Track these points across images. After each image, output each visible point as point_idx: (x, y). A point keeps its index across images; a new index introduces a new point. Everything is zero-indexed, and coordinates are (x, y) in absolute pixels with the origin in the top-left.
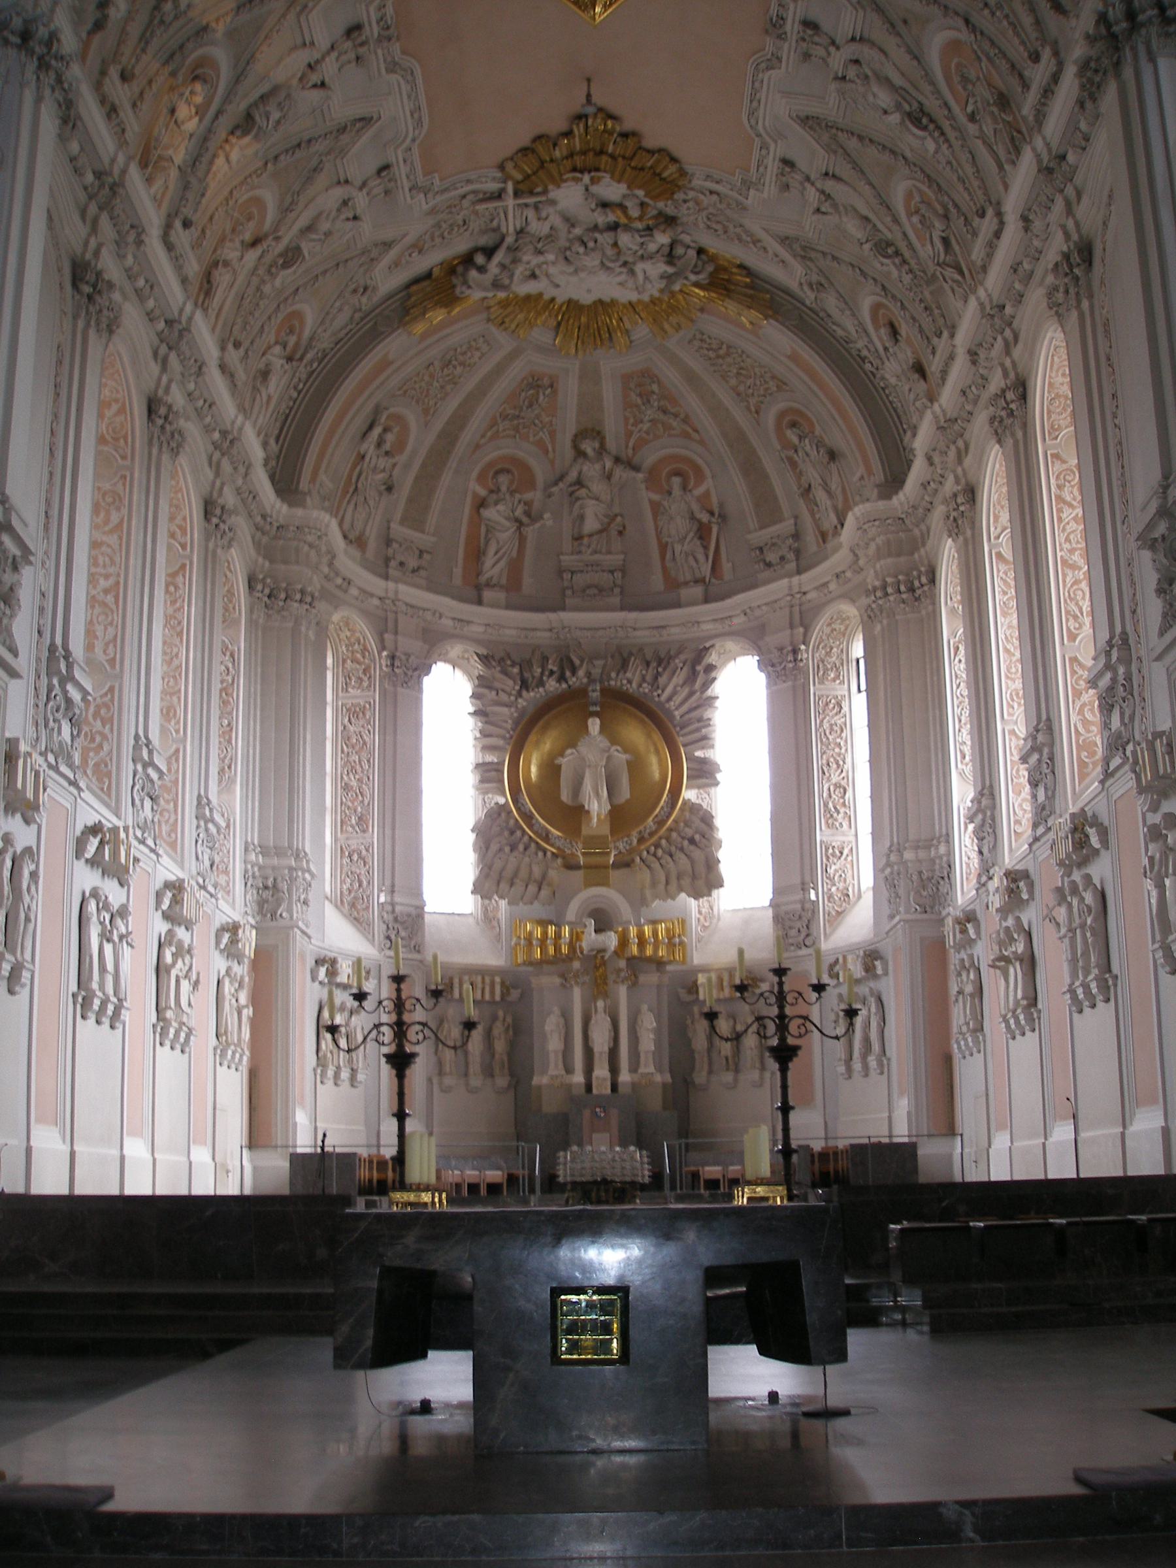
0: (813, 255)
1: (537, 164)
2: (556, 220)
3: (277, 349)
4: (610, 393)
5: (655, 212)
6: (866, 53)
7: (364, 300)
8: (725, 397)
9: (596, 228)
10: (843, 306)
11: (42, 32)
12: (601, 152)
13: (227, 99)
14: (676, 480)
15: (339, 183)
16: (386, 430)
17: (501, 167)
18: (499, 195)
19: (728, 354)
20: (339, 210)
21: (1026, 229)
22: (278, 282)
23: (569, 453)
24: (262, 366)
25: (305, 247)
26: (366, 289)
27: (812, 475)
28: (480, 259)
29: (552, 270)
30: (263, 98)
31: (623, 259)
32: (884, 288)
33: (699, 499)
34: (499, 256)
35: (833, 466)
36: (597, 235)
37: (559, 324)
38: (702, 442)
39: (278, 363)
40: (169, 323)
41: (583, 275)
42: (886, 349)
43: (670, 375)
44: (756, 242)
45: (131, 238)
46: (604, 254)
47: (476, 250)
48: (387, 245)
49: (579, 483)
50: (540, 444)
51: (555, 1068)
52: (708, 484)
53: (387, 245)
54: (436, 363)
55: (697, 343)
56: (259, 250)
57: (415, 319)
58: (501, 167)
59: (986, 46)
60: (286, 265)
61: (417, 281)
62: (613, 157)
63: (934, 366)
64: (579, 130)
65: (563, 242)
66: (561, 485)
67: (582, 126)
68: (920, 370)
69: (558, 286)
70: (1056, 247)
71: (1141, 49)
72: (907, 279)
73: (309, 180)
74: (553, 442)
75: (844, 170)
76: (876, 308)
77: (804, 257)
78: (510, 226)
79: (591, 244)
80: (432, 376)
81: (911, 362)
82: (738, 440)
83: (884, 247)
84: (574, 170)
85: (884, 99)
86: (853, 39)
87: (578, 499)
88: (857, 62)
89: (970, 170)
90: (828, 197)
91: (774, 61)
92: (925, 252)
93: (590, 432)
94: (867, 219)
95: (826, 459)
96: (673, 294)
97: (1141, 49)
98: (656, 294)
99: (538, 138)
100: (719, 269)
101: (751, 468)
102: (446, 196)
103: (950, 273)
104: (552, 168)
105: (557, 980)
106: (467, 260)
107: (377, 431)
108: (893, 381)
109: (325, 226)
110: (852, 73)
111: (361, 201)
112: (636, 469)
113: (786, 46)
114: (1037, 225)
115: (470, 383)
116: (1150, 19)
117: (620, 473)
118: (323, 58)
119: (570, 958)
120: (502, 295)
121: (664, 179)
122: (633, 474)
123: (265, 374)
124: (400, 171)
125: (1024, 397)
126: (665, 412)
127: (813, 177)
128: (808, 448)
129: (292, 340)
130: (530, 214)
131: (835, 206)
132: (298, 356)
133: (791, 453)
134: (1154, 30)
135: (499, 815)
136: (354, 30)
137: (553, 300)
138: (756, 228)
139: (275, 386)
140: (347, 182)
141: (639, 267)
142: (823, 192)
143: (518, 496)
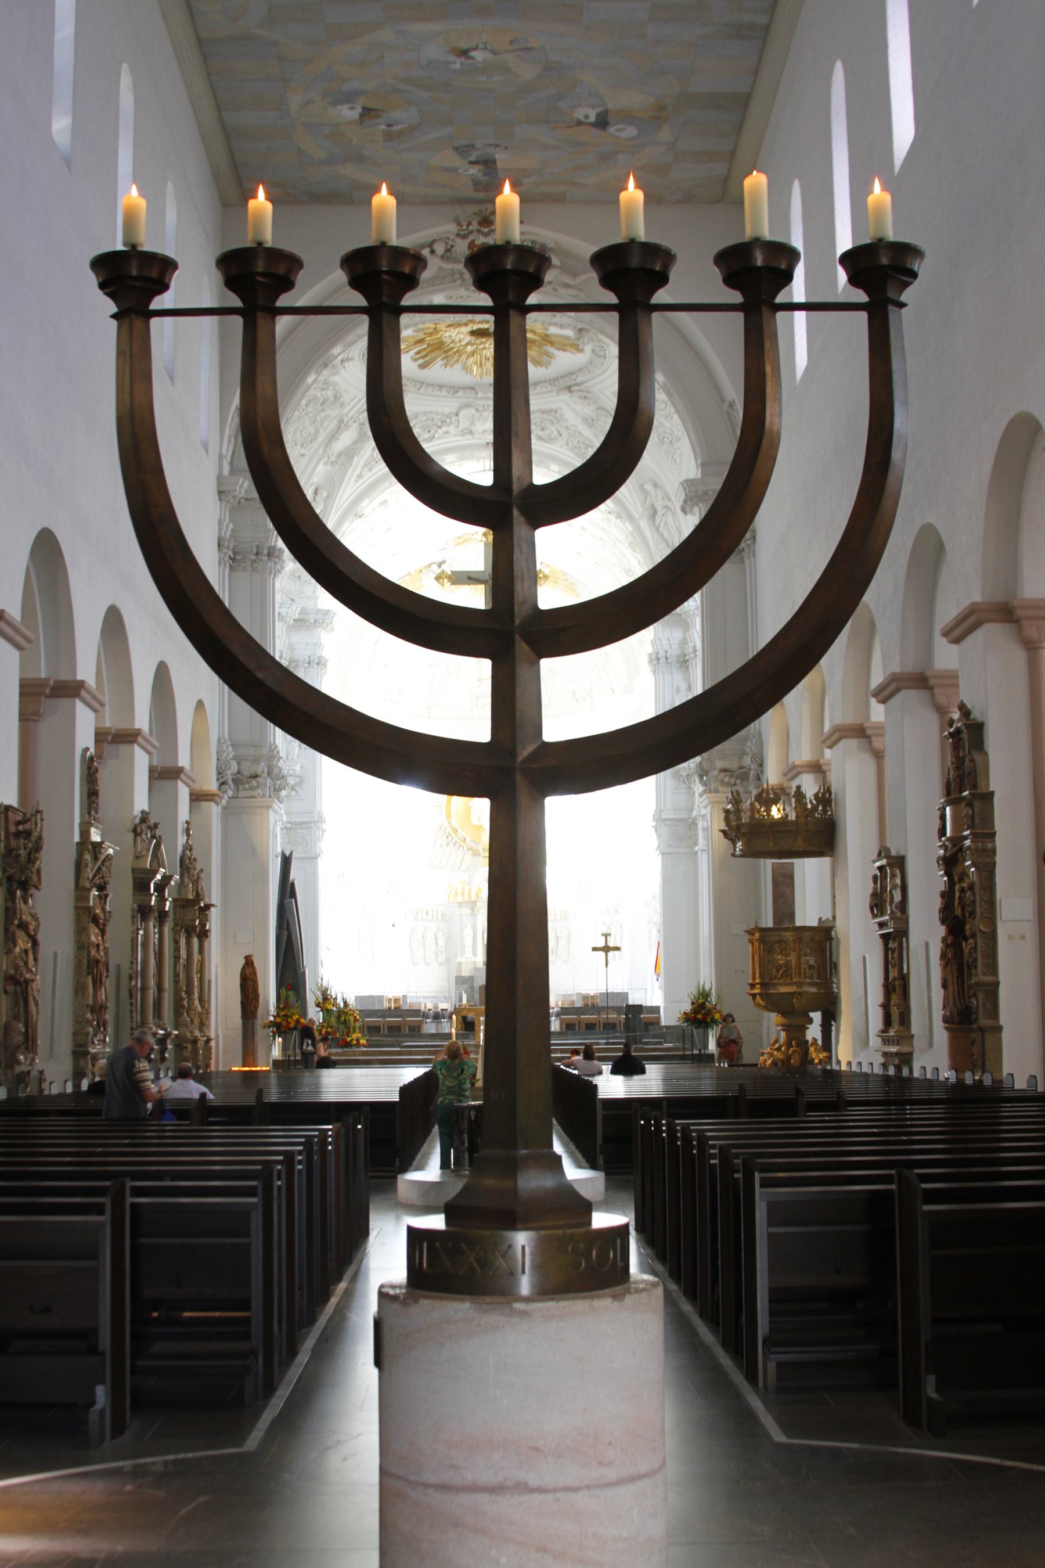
47: (433, 563)
51: (469, 953)
71: (660, 669)
97: (660, 669)
105: (470, 911)
119: (475, 902)
135: (441, 828)
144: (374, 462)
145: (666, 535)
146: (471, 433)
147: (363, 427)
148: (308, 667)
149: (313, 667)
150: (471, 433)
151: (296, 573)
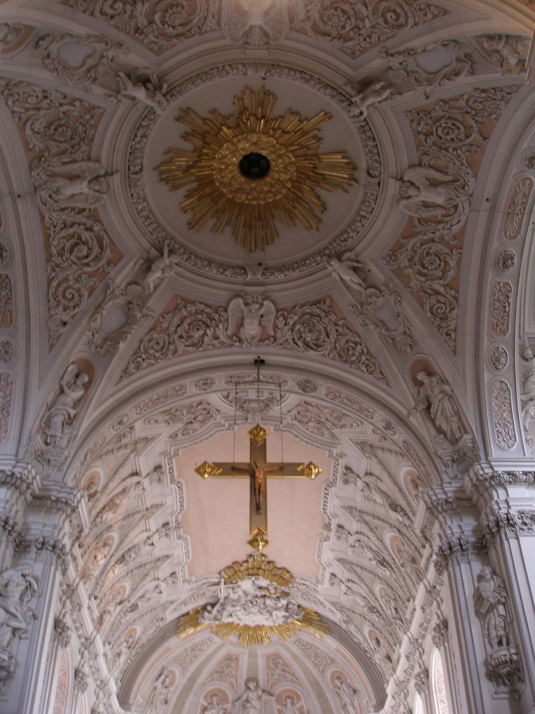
0: (344, 610)
1: (234, 572)
2: (240, 593)
3: (125, 644)
4: (261, 663)
5: (280, 591)
6: (362, 537)
7: (161, 623)
8: (310, 666)
9: (257, 596)
10: (357, 630)
11: (60, 546)
12: (260, 568)
13: (116, 551)
14: (289, 701)
15: (155, 579)
16: (166, 677)
17: (220, 573)
18: (218, 584)
19: (311, 648)
20: (154, 590)
21: (424, 612)
22: (128, 618)
23: (243, 687)
24: (118, 651)
25: (140, 605)
26: (162, 619)
27: (347, 700)
28: (209, 608)
29: (238, 613)
30: (129, 550)
31: (267, 609)
32: (373, 624)
33: (298, 709)
34: (217, 607)
35: (355, 697)
36: (257, 599)
37: (240, 634)
38: (300, 684)
39: (124, 650)
40: (86, 639)
41: (251, 615)
42: (375, 649)
43: (287, 656)
44: (322, 603)
45: (78, 608)
46: (260, 607)
47: (208, 604)
48: (172, 602)
49: (247, 701)
50: (231, 684)
52: (303, 702)
53: (172, 602)
54: (189, 649)
55: (298, 643)
56: (122, 606)
57: (181, 632)
58: (220, 573)
59: (406, 540)
60: (131, 611)
61: (183, 616)
62: (264, 570)
63: (394, 657)
64: (251, 560)
65: (243, 601)
66: (239, 701)
67: (252, 559)
68: (389, 658)
69: (240, 620)
70: (435, 621)
71: (455, 560)
72: (382, 622)
73: (144, 578)
74: (236, 682)
75: (356, 579)
76: (370, 632)
77: (341, 611)
78: (222, 596)
79: (255, 603)
80: (187, 655)
81: (385, 654)
82: (315, 684)
83: (372, 609)
84: (249, 575)
85: (370, 555)
86: (357, 533)
87: (246, 708)
88: (359, 541)
89: (403, 584)
90: (350, 588)
91: (327, 539)
92: (389, 612)
93: (252, 679)
94: (365, 598)
95: (352, 693)
96: (288, 624)
97: (455, 560)
98: (281, 623)
99: (235, 563)
100: (307, 613)
101: (321, 695)
102: (197, 584)
103: (398, 622)
104: (240, 574)
106: (204, 608)
107: (163, 677)
108: (378, 662)
109: (148, 596)
110: (357, 545)
111: (163, 585)
112: (272, 695)
113: (331, 534)
114: (428, 611)
115: (202, 657)
116: (457, 550)
117: (265, 697)
118: (153, 534)
120: (217, 623)
121: (284, 579)
122: (270, 697)
123: (119, 655)
124: (180, 575)
125: (428, 676)
126: (284, 671)
127: (343, 580)
128: (345, 688)
129: (131, 640)
130: (230, 591)
131: (352, 592)
132: (132, 646)
133: (338, 690)
134: (459, 554)
136: (166, 525)
137: (238, 625)
138: (322, 599)
139: (123, 659)
140: (158, 579)
141: (274, 613)
142: (348, 587)
143: (220, 706)
144: (141, 360)
145: (444, 426)
146: (240, 341)
147: (131, 306)
148: (41, 549)
149: (47, 549)
150: (240, 341)
151: (45, 455)
